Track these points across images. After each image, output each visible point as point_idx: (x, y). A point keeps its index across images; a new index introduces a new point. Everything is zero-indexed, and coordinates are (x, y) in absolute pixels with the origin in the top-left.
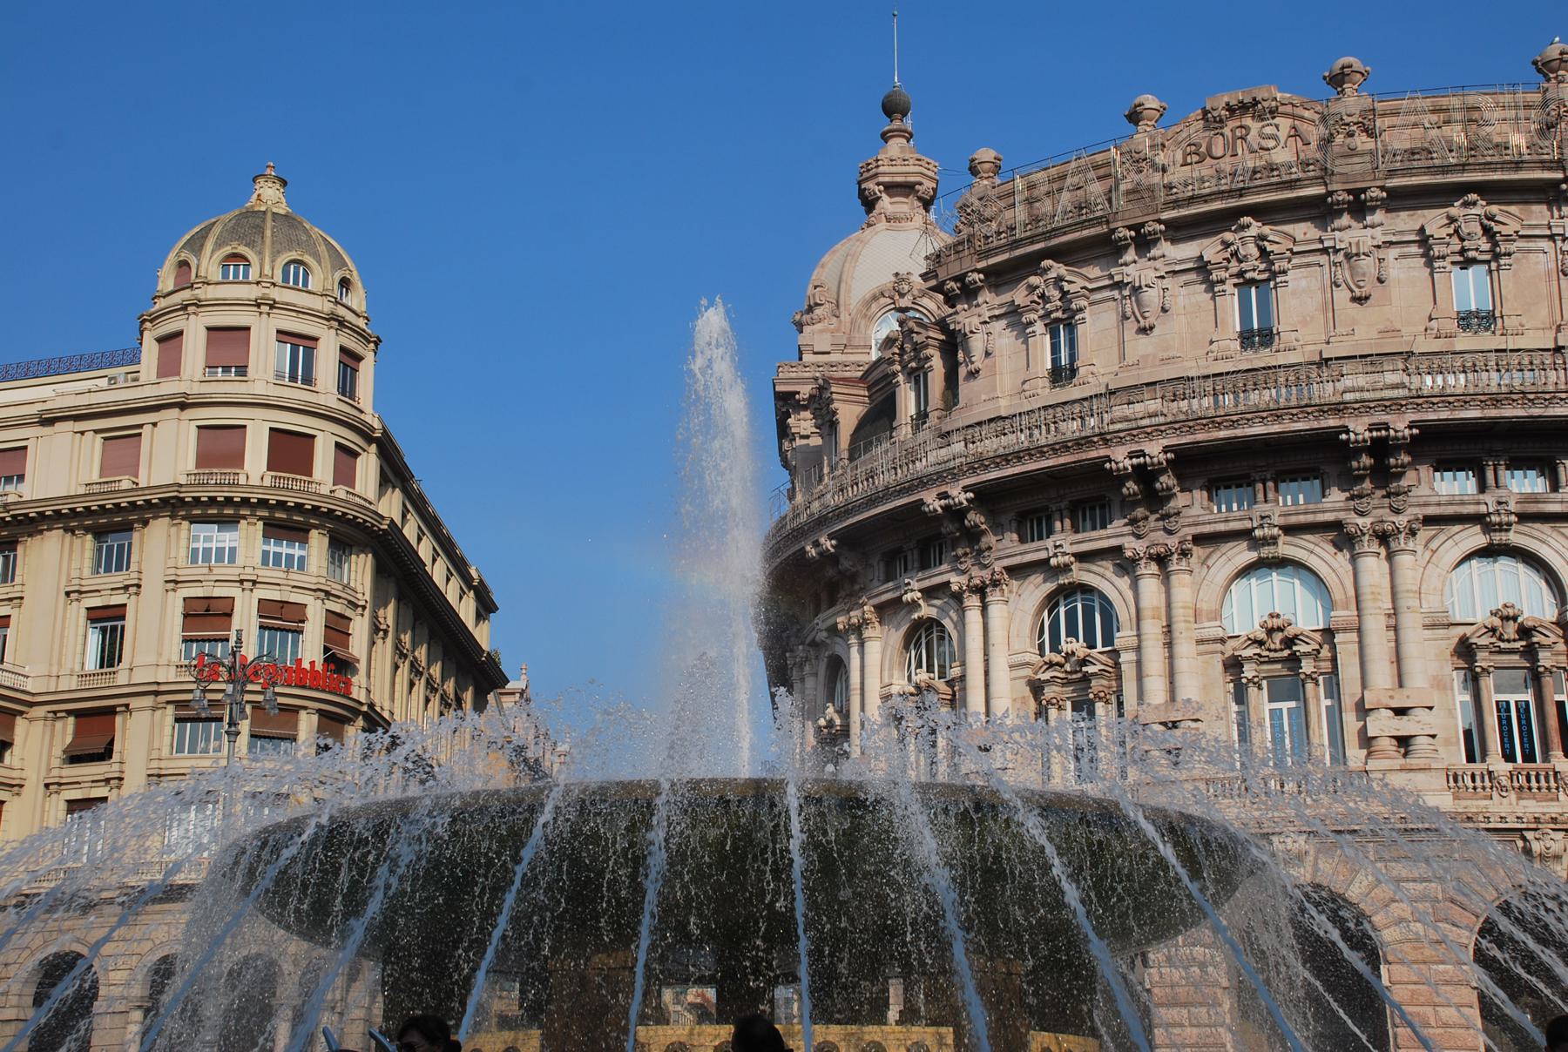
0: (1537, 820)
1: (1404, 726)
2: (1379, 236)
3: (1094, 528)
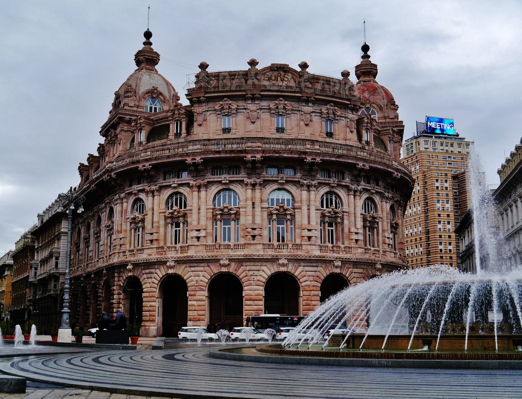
0: (336, 258)
3: (233, 174)
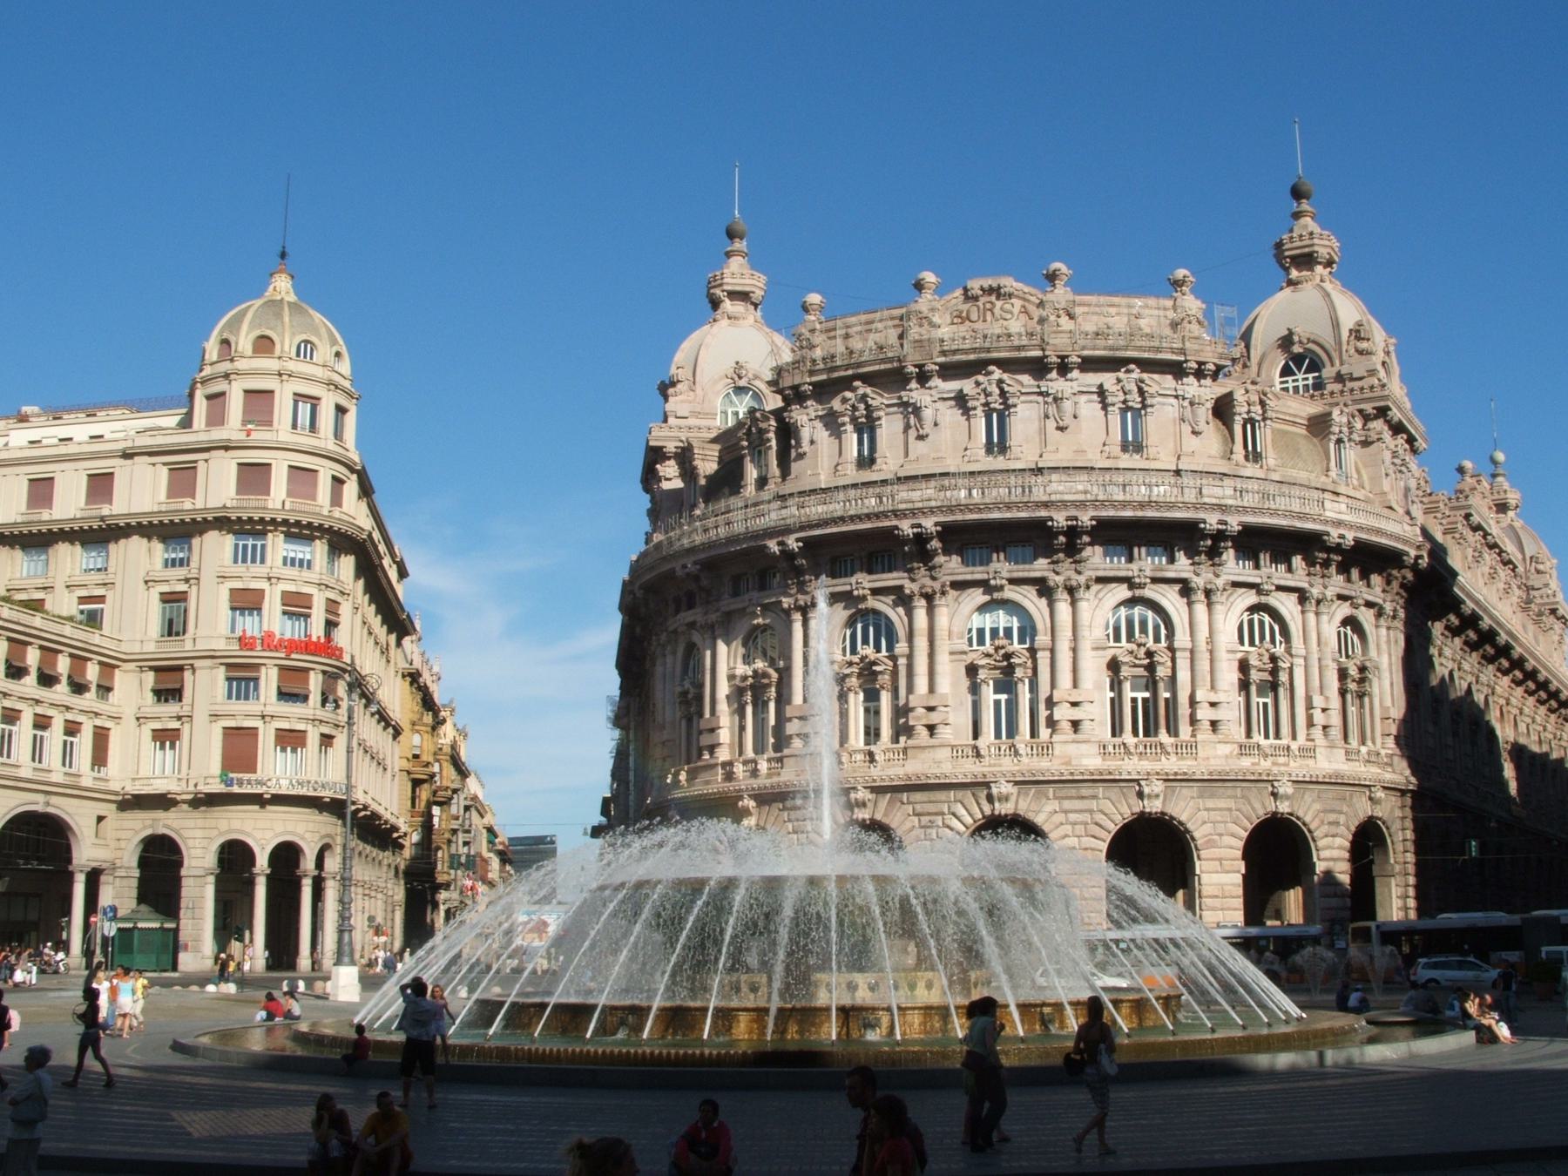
1: (1076, 714)
2: (1076, 387)
